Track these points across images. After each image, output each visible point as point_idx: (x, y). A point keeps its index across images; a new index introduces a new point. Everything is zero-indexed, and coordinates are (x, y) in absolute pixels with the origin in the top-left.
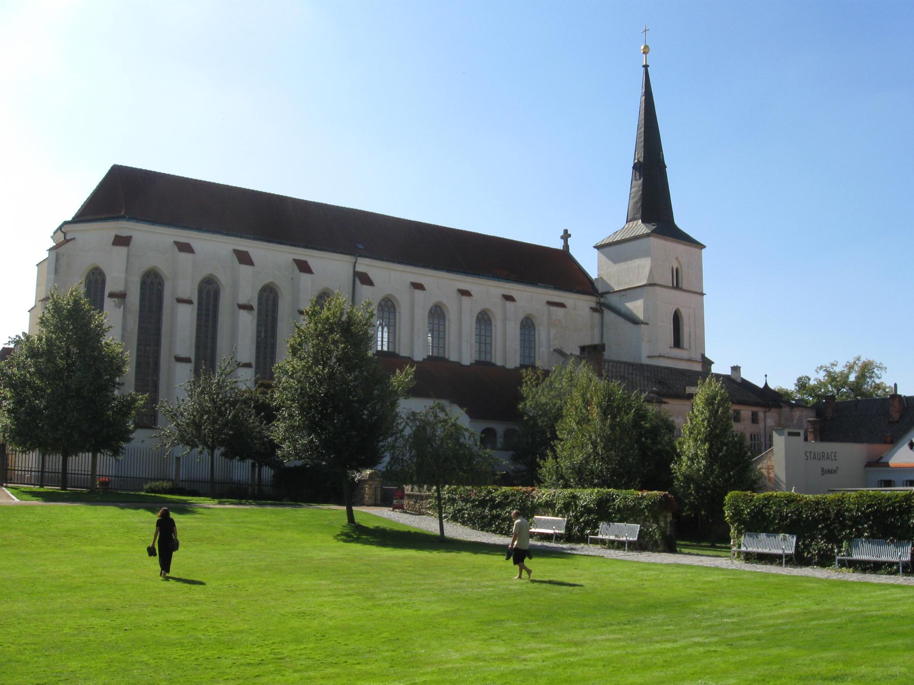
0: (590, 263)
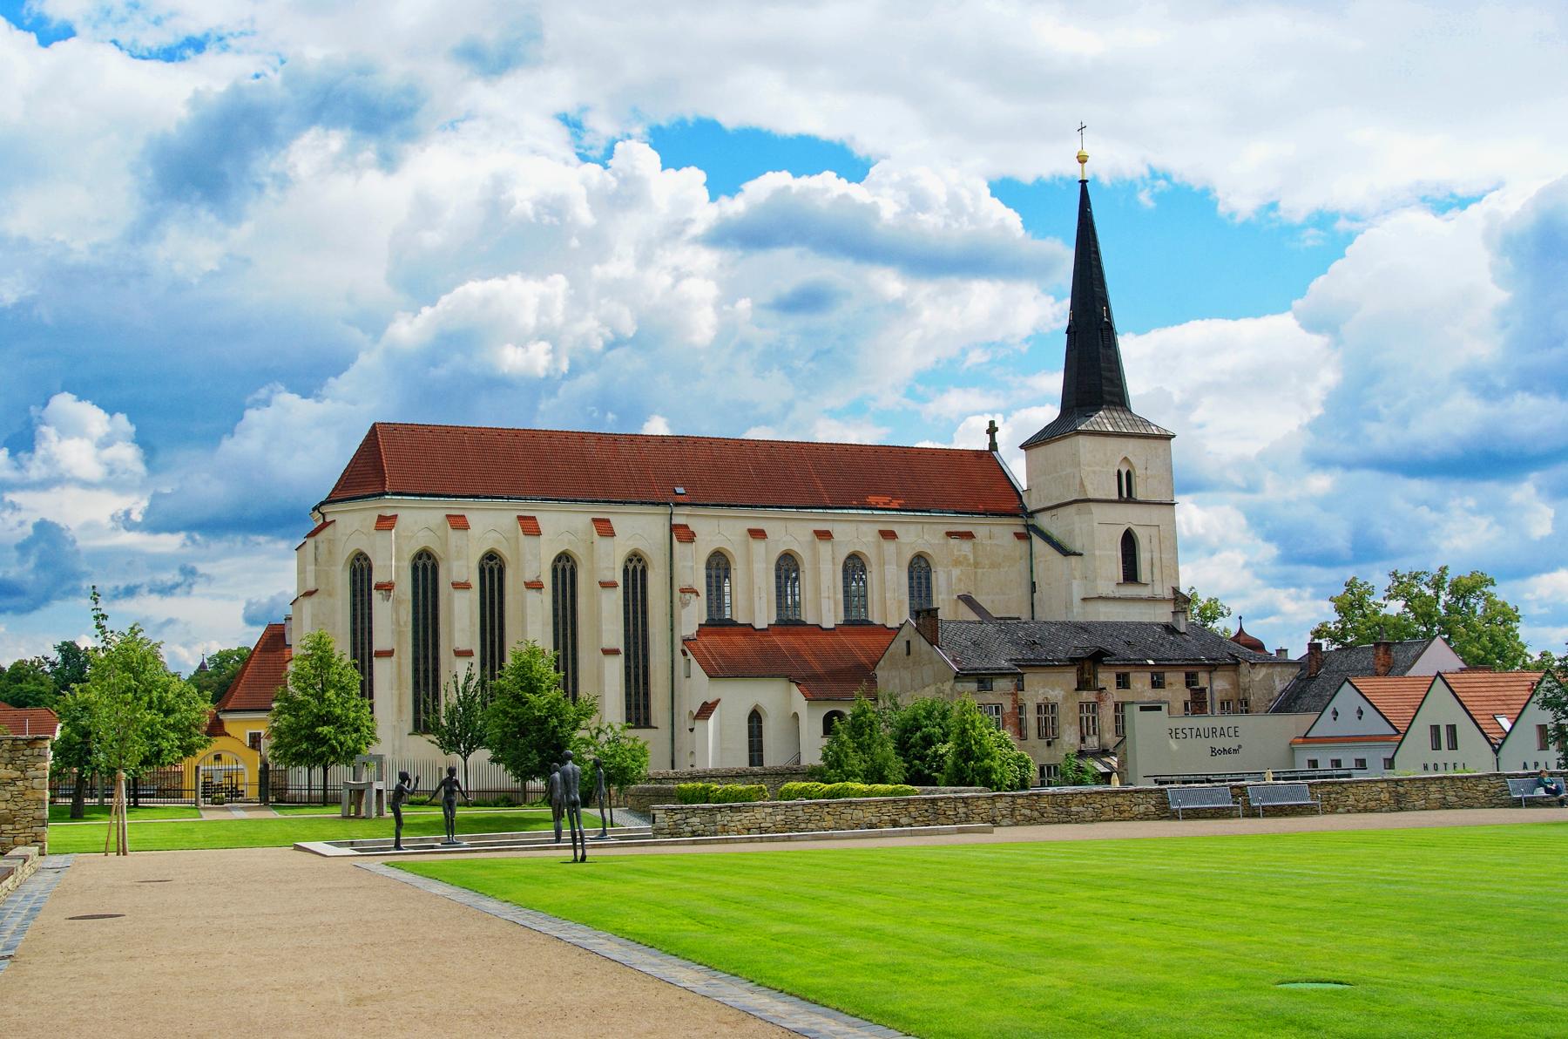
0: (1017, 468)
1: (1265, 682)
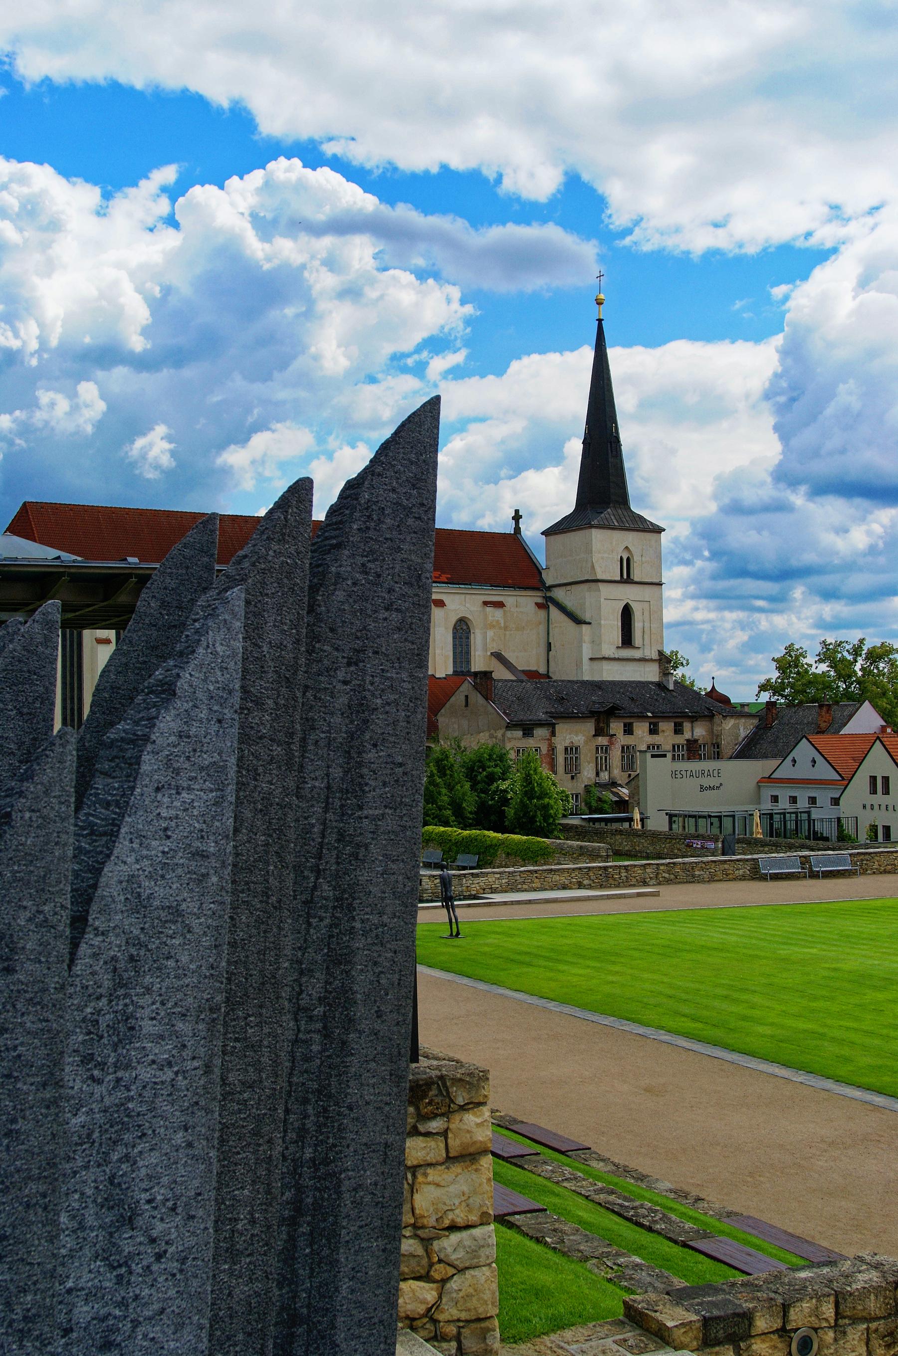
1: (735, 731)
